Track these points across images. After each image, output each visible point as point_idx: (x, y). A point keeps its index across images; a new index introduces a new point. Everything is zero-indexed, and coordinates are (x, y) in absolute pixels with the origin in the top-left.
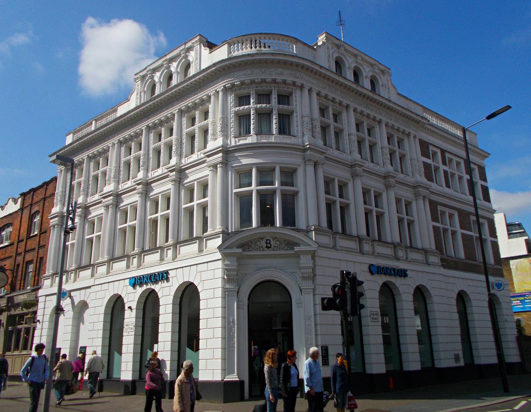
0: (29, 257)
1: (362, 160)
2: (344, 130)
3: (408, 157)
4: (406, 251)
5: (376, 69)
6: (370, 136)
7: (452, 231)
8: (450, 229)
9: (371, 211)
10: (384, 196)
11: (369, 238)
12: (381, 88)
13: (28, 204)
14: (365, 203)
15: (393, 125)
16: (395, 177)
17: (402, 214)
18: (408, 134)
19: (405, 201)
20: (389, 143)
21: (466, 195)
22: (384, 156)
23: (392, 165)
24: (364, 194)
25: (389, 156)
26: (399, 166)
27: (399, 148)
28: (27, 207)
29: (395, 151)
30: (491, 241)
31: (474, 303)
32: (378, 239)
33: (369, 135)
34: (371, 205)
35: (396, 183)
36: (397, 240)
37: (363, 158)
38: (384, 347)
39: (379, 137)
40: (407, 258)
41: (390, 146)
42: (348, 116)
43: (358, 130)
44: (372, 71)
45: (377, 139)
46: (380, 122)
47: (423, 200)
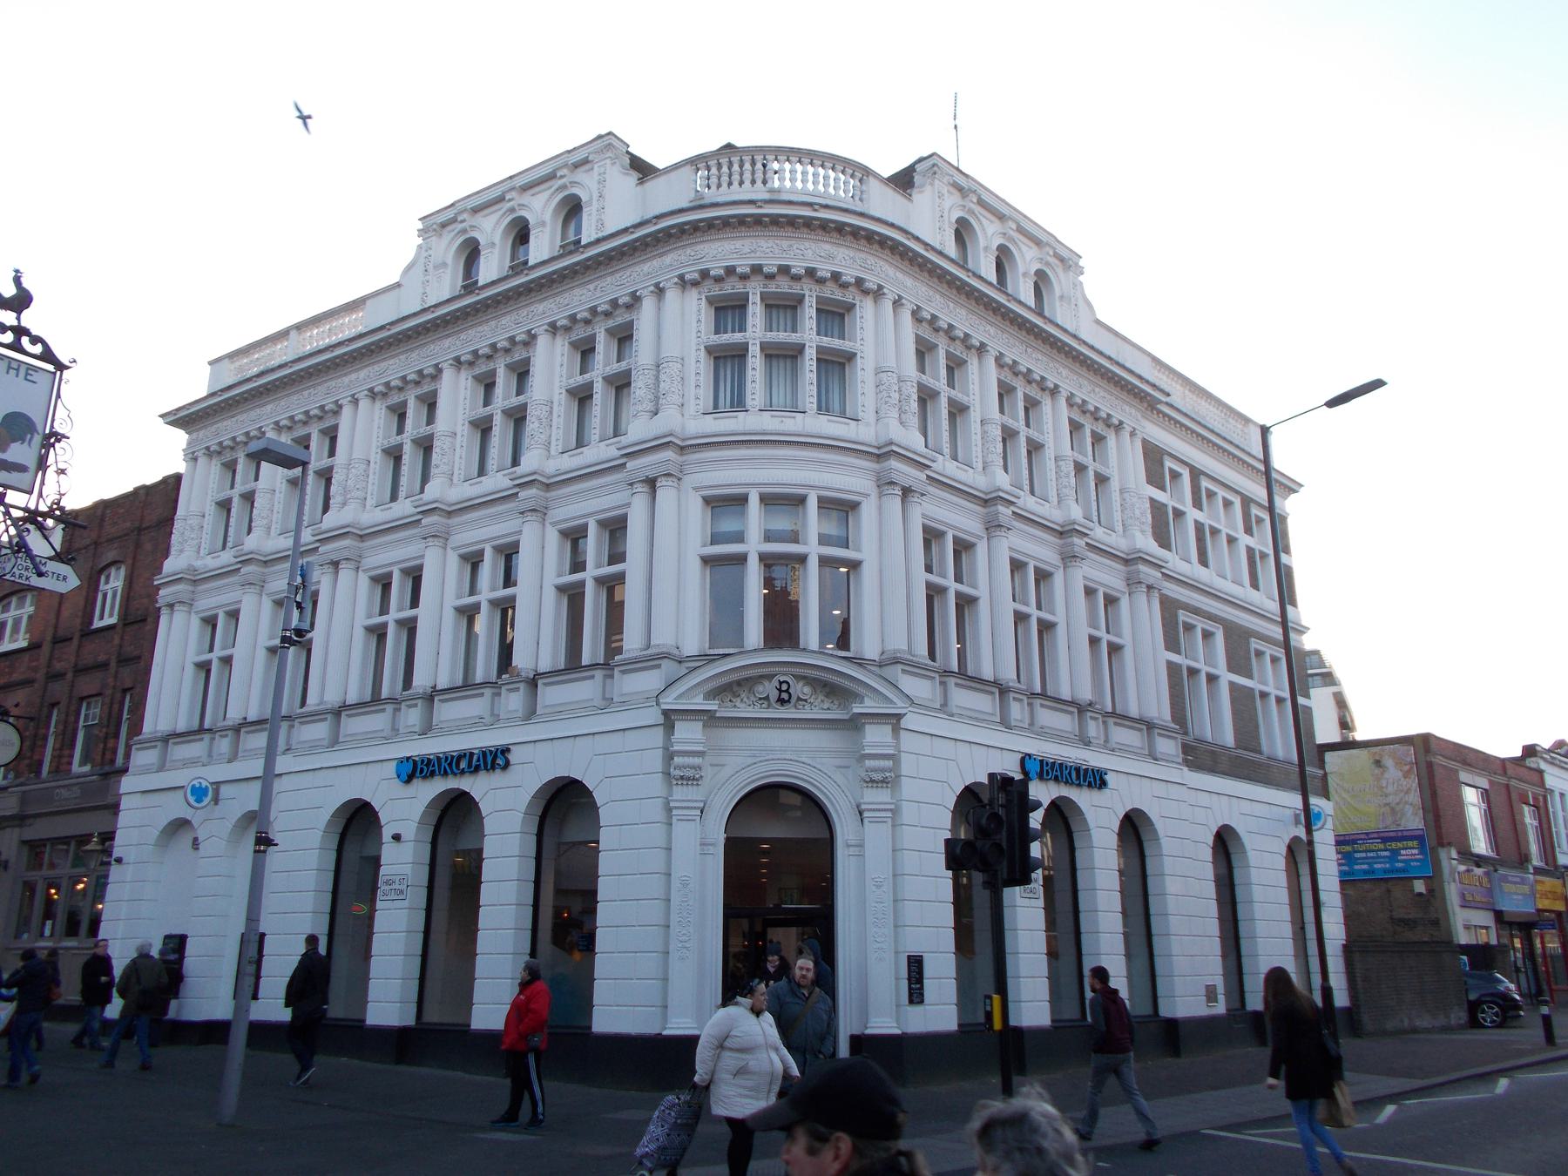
0: (88, 684)
3: (1115, 484)
4: (943, 683)
5: (1050, 256)
6: (924, 373)
11: (935, 664)
12: (982, 254)
13: (88, 541)
14: (929, 569)
15: (967, 335)
16: (1012, 503)
17: (1026, 604)
18: (978, 349)
20: (1002, 411)
23: (1006, 471)
24: (927, 544)
26: (1025, 473)
27: (1028, 425)
28: (86, 548)
31: (1167, 845)
32: (959, 669)
33: (951, 384)
34: (944, 576)
37: (930, 447)
38: (956, 959)
39: (977, 393)
40: (945, 704)
41: (1031, 431)
43: (922, 369)
45: (972, 396)
46: (981, 349)
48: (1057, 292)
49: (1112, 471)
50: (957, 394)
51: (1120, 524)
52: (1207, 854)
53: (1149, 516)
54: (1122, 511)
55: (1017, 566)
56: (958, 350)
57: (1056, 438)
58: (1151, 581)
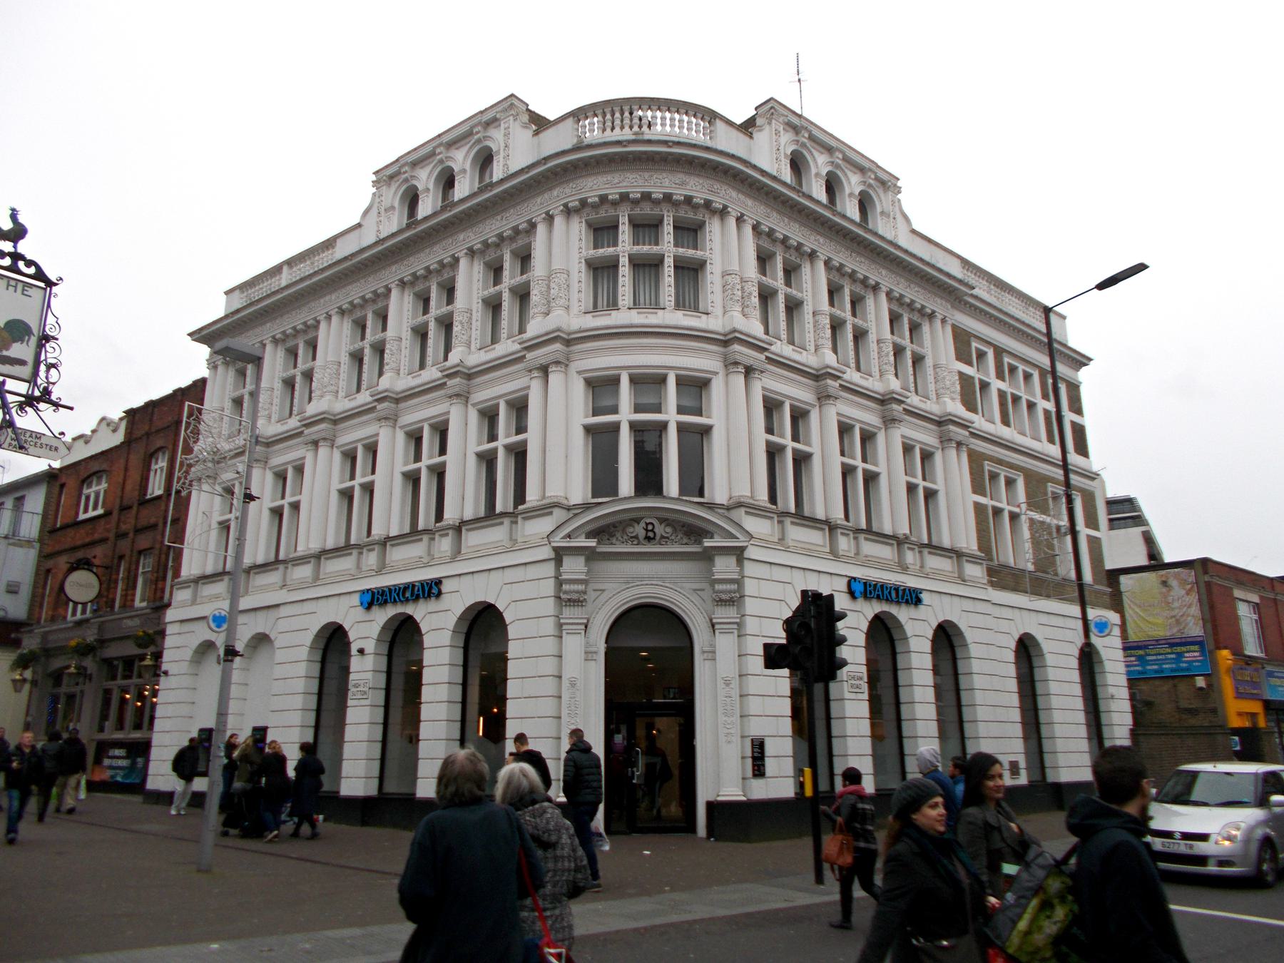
1: (768, 337)
2: (708, 262)
3: (929, 362)
7: (925, 489)
8: (790, 445)
9: (782, 448)
10: (814, 416)
19: (793, 408)
21: (994, 423)
22: (818, 332)
25: (829, 331)
29: (845, 322)
30: (1088, 536)
35: (768, 363)
36: (838, 514)
42: (723, 234)
44: (793, 141)
47: (745, 377)
48: (879, 209)
49: (927, 350)
50: (859, 322)
51: (934, 392)
52: (1011, 656)
53: (958, 388)
54: (935, 383)
55: (908, 449)
56: (916, 317)
57: (877, 325)
58: (959, 438)
